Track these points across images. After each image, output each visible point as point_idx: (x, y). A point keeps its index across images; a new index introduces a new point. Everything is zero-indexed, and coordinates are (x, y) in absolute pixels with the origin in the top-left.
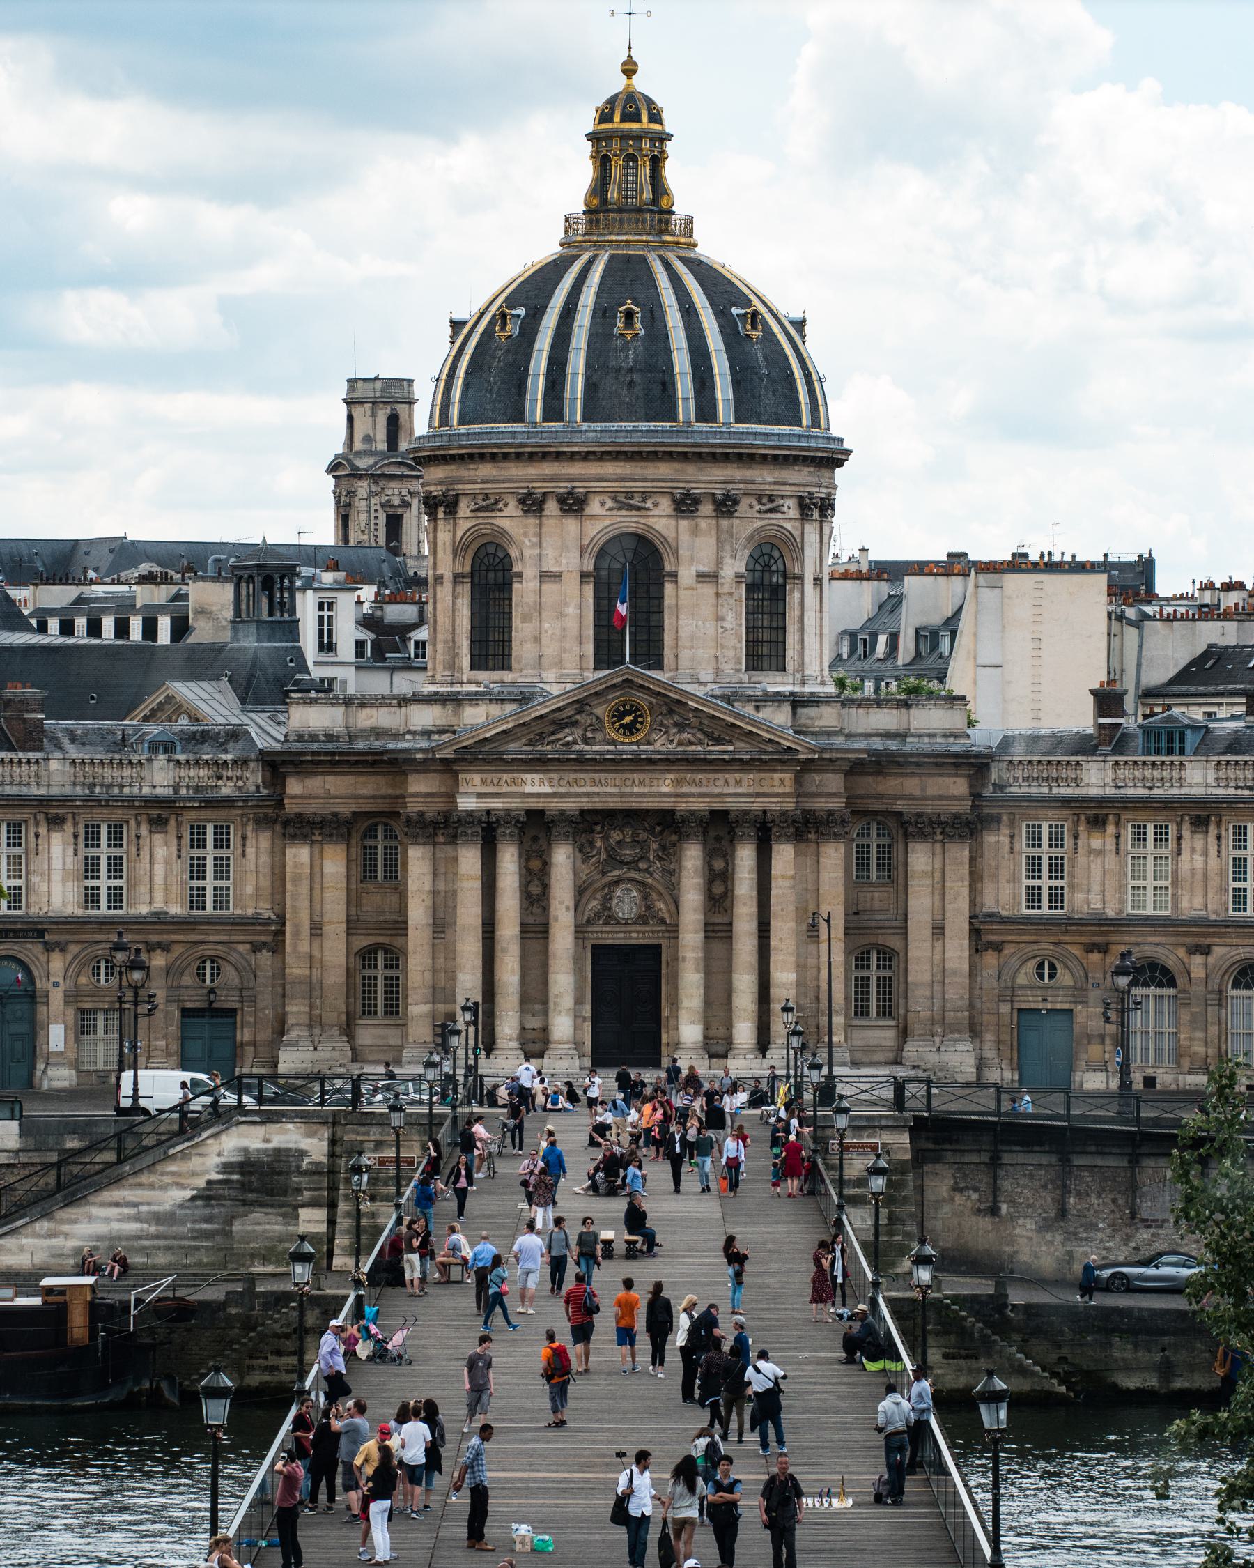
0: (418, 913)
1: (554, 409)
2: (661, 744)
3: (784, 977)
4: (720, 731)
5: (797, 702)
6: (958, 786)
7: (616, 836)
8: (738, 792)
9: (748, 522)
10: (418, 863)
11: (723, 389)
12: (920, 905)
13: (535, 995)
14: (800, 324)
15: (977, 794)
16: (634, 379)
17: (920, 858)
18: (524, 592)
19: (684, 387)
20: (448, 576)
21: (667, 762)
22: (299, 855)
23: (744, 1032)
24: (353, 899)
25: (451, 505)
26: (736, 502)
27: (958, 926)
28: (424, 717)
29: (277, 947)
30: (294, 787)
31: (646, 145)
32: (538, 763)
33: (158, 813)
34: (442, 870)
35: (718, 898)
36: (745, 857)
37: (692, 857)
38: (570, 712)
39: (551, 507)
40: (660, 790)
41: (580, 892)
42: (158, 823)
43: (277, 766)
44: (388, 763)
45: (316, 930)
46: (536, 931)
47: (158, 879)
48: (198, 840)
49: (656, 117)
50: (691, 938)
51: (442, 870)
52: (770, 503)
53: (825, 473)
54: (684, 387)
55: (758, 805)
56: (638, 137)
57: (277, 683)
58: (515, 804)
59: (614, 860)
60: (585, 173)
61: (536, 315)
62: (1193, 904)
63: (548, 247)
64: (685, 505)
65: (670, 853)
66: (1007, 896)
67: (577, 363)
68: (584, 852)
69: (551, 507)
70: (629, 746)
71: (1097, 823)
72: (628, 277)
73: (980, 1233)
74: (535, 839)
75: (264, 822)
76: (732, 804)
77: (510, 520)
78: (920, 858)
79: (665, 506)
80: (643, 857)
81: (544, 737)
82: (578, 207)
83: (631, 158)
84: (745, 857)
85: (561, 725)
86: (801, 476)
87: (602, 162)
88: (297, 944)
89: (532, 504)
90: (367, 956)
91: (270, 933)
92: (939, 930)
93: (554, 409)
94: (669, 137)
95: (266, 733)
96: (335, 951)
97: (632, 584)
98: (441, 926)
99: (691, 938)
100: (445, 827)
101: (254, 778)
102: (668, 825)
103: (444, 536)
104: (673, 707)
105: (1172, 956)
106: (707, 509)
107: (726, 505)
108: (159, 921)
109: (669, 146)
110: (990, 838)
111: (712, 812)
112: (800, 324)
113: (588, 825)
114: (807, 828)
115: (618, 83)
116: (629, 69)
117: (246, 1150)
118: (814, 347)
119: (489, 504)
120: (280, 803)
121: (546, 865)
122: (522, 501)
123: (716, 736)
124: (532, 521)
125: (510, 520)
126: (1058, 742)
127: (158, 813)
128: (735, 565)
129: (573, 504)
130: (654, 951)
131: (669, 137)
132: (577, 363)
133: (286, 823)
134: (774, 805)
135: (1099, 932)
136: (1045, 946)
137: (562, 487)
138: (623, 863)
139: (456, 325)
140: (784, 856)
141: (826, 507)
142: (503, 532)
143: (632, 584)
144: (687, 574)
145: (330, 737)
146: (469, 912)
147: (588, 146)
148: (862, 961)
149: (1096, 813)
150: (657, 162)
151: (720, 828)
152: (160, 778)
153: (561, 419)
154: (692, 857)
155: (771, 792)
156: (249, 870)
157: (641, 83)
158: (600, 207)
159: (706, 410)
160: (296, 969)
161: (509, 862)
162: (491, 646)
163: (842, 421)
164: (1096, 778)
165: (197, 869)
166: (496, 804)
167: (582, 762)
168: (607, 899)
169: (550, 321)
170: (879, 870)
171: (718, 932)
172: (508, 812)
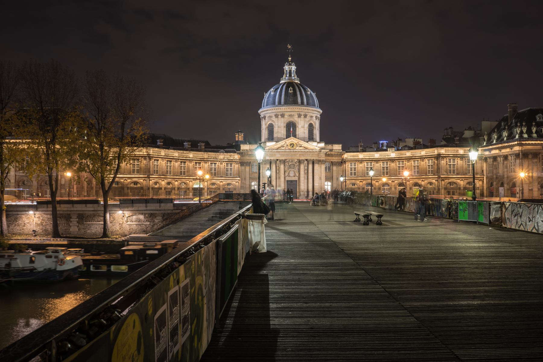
1: (280, 103)
37: (302, 166)
39: (280, 116)
52: (312, 117)
55: (312, 158)
58: (275, 158)
59: (290, 167)
64: (299, 116)
69: (280, 116)
76: (309, 158)
77: (274, 118)
79: (297, 116)
84: (310, 166)
89: (277, 116)
99: (302, 179)
107: (305, 116)
117: (220, 210)
128: (307, 126)
129: (283, 116)
134: (315, 158)
140: (316, 166)
142: (273, 121)
144: (300, 126)
145: (247, 150)
159: (302, 103)
166: (272, 158)
168: (289, 173)
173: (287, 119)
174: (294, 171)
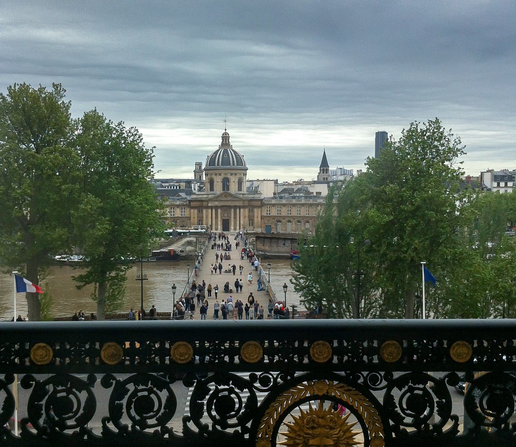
0: (204, 216)
1: (218, 165)
2: (229, 199)
3: (242, 222)
4: (236, 197)
5: (243, 194)
6: (260, 203)
8: (237, 204)
9: (238, 176)
10: (204, 211)
11: (235, 163)
12: (256, 214)
13: (217, 224)
15: (262, 203)
16: (226, 161)
17: (256, 210)
18: (215, 183)
19: (231, 162)
21: (230, 200)
22: (192, 210)
23: (238, 228)
24: (198, 215)
25: (208, 175)
27: (259, 217)
28: (205, 196)
29: (190, 220)
30: (192, 203)
32: (217, 201)
33: (178, 206)
34: (207, 212)
35: (235, 214)
36: (238, 210)
40: (229, 204)
42: (178, 207)
43: (190, 201)
44: (202, 201)
45: (194, 218)
46: (216, 218)
47: (178, 213)
48: (182, 209)
50: (232, 218)
51: (207, 212)
52: (240, 174)
54: (231, 162)
57: (190, 193)
60: (221, 141)
61: (216, 155)
62: (283, 214)
63: (217, 148)
64: (231, 174)
65: (230, 210)
66: (264, 214)
67: (221, 160)
70: (226, 199)
71: (274, 206)
72: (226, 151)
73: (263, 248)
77: (214, 176)
78: (256, 210)
81: (216, 198)
82: (220, 144)
84: (238, 210)
86: (243, 171)
87: (223, 140)
88: (192, 219)
89: (216, 175)
90: (199, 221)
91: (189, 218)
92: (258, 217)
93: (218, 165)
95: (189, 198)
96: (196, 220)
97: (226, 183)
98: (207, 217)
99: (232, 218)
100: (207, 207)
101: (188, 203)
102: (230, 207)
104: (231, 195)
105: (281, 220)
107: (236, 174)
108: (178, 217)
110: (263, 208)
113: (222, 207)
114: (244, 207)
119: (212, 174)
123: (235, 197)
125: (214, 176)
126: (269, 198)
127: (178, 206)
128: (237, 181)
129: (220, 174)
132: (221, 160)
135: (274, 217)
136: (268, 219)
140: (242, 210)
141: (246, 174)
143: (226, 183)
144: (232, 181)
146: (210, 216)
148: (250, 220)
149: (274, 205)
150: (228, 140)
151: (235, 207)
152: (178, 203)
154: (233, 210)
155: (240, 204)
156: (187, 212)
157: (227, 131)
158: (223, 144)
159: (234, 165)
160: (192, 222)
161: (214, 211)
162: (212, 189)
164: (274, 202)
165: (182, 212)
167: (221, 201)
169: (218, 156)
170: (251, 211)
171: (235, 218)
173: (223, 176)
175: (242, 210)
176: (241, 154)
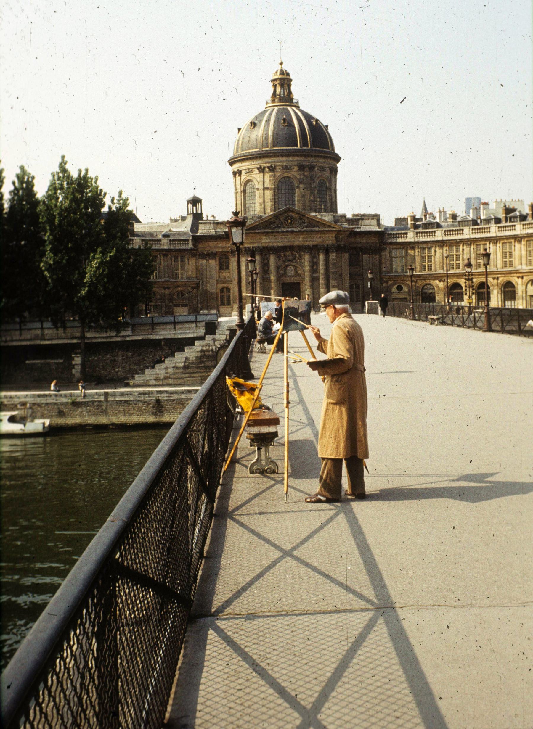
7: (287, 253)
14: (327, 126)
20: (239, 190)
26: (314, 168)
31: (286, 82)
32: (266, 234)
38: (274, 219)
40: (300, 240)
41: (278, 268)
49: (288, 74)
53: (334, 162)
56: (284, 79)
58: (260, 245)
65: (301, 257)
68: (279, 257)
74: (266, 255)
75: (194, 255)
79: (296, 168)
80: (295, 259)
83: (282, 85)
84: (322, 257)
85: (271, 223)
87: (275, 86)
89: (261, 170)
94: (291, 80)
102: (302, 249)
103: (238, 182)
106: (307, 169)
109: (292, 83)
110: (383, 253)
111: (313, 246)
112: (327, 126)
114: (339, 249)
115: (279, 67)
116: (281, 64)
118: (330, 130)
119: (250, 171)
120: (197, 250)
121: (268, 261)
122: (258, 169)
124: (262, 174)
129: (272, 169)
130: (299, 284)
131: (291, 80)
133: (200, 255)
137: (269, 165)
138: (289, 261)
139: (239, 129)
140: (333, 256)
141: (334, 171)
147: (272, 84)
150: (289, 86)
153: (268, 147)
155: (329, 240)
157: (285, 67)
163: (338, 150)
168: (286, 270)
172: (258, 247)
174: (293, 266)
175: (333, 256)
176: (324, 121)
